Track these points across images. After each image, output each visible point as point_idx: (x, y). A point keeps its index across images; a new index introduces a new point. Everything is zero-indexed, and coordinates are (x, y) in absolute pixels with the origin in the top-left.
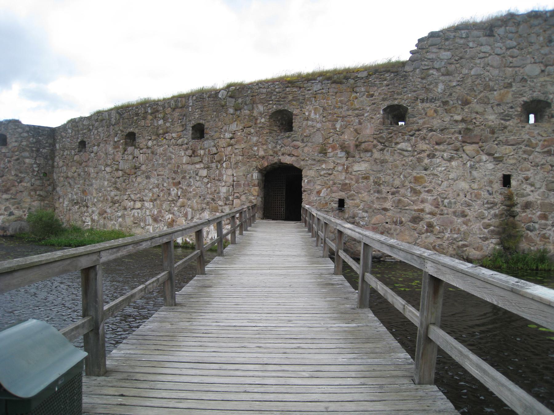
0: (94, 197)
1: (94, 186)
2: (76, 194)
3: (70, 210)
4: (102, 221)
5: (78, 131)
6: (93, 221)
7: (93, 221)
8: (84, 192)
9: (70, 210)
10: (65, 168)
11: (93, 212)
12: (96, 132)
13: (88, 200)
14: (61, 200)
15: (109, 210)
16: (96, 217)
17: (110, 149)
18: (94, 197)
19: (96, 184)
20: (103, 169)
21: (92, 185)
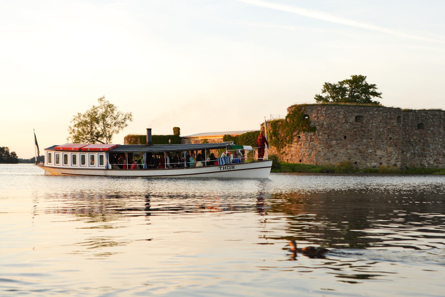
0: (431, 153)
1: (431, 147)
2: (417, 150)
3: (412, 158)
4: (435, 165)
5: (418, 118)
6: (429, 164)
7: (429, 164)
8: (424, 150)
9: (412, 158)
10: (407, 136)
11: (429, 160)
12: (431, 121)
13: (426, 154)
14: (405, 153)
15: (441, 159)
16: (432, 162)
17: (441, 130)
18: (431, 153)
19: (432, 146)
20: (437, 139)
21: (429, 146)
